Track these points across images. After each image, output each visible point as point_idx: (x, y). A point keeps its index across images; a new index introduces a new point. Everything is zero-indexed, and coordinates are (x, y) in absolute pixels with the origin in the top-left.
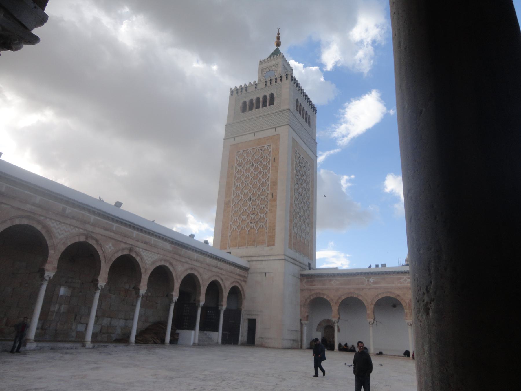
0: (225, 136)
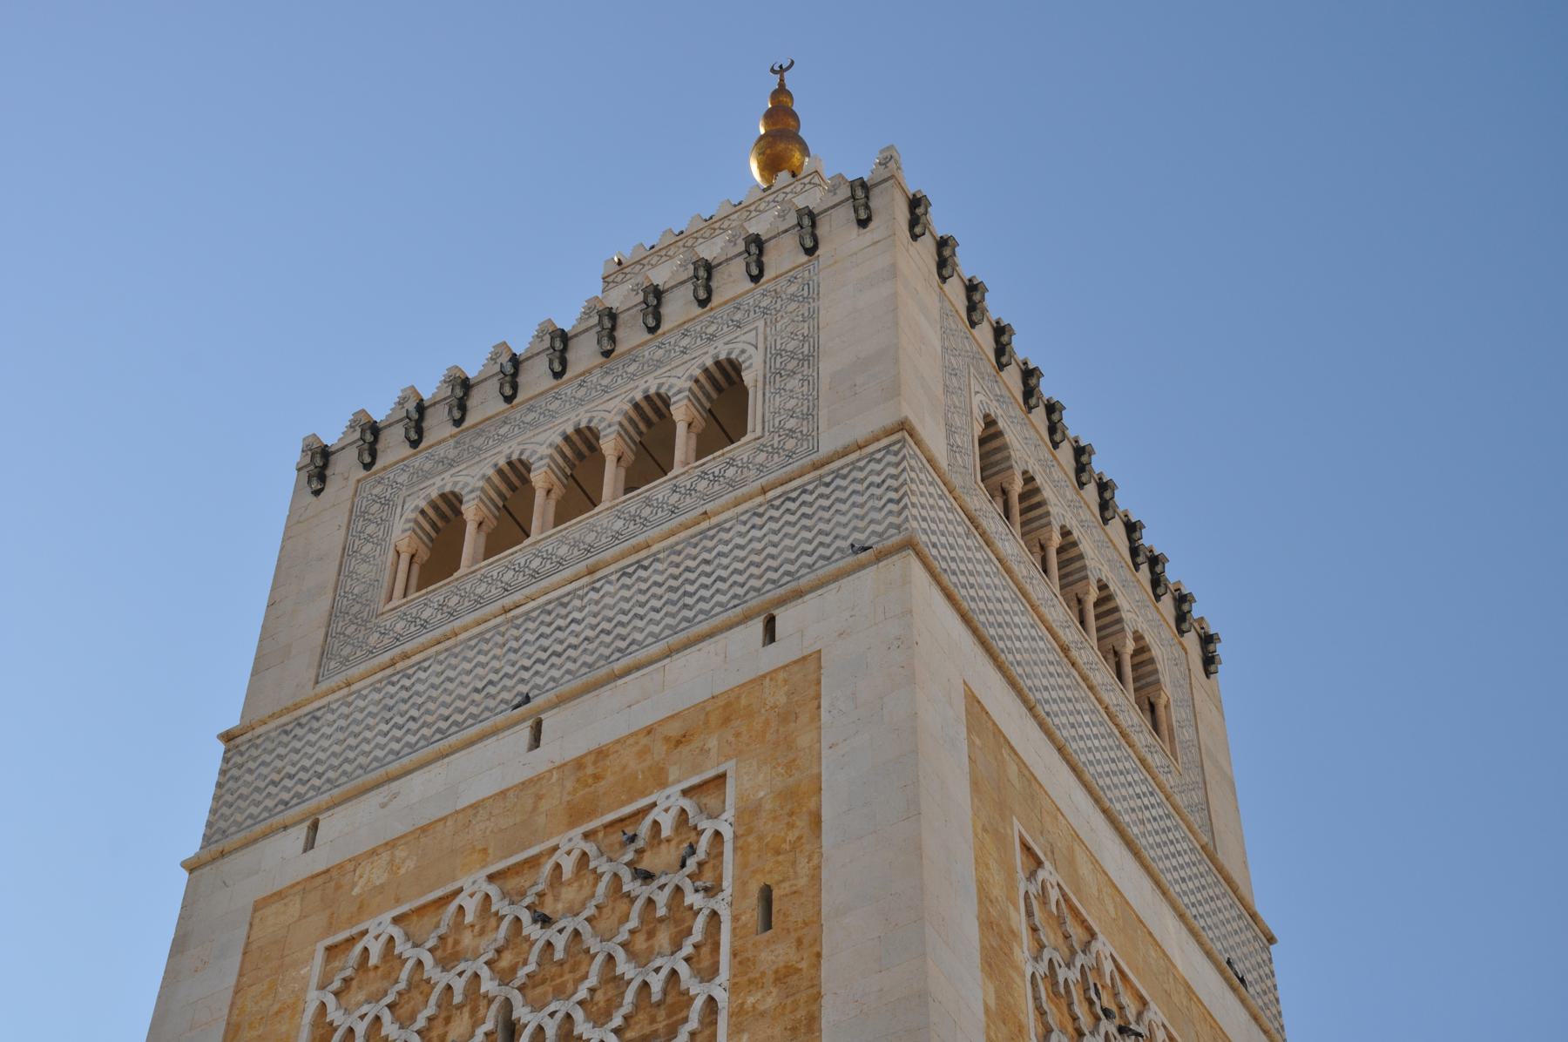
0: (207, 839)
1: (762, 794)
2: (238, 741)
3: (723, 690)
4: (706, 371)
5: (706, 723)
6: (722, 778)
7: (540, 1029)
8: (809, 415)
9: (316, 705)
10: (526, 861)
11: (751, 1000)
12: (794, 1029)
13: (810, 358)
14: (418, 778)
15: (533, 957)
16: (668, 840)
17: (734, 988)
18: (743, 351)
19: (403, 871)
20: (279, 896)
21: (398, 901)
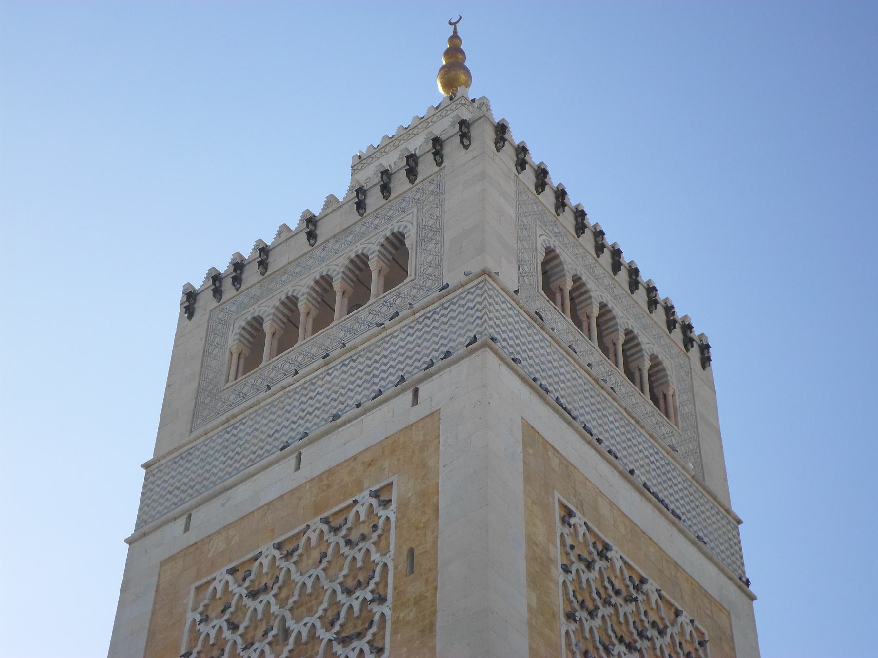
1: (410, 495)
2: (152, 468)
3: (391, 433)
4: (387, 239)
5: (383, 452)
6: (390, 485)
7: (299, 633)
8: (439, 266)
9: (190, 446)
10: (293, 536)
11: (402, 615)
12: (423, 631)
13: (439, 231)
14: (240, 489)
15: (296, 592)
16: (364, 522)
17: (394, 608)
18: (406, 227)
19: (233, 543)
20: (172, 558)
21: (231, 560)
